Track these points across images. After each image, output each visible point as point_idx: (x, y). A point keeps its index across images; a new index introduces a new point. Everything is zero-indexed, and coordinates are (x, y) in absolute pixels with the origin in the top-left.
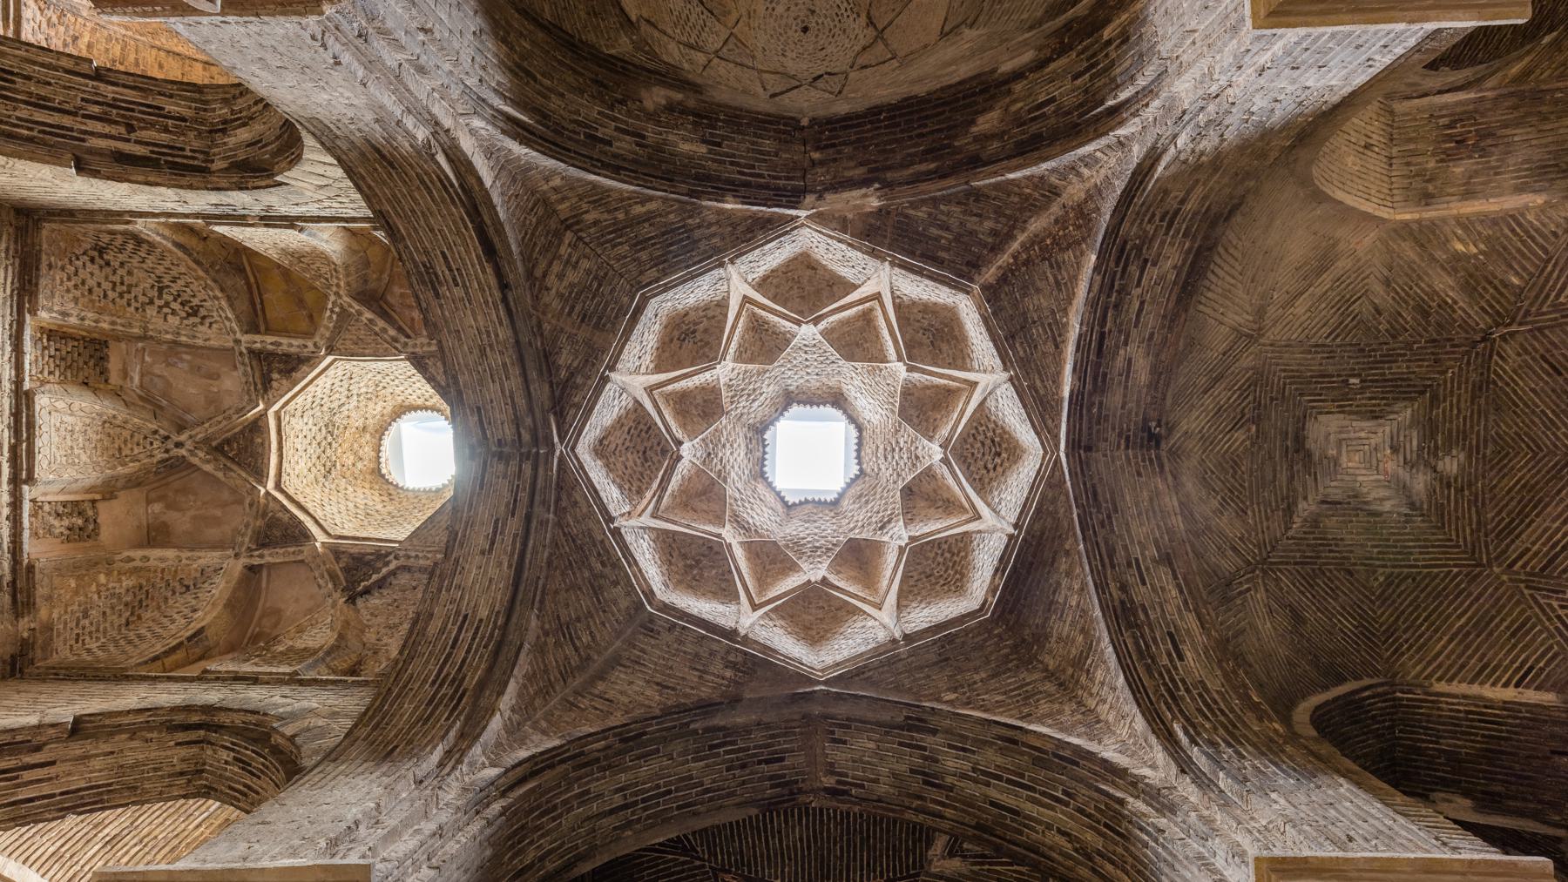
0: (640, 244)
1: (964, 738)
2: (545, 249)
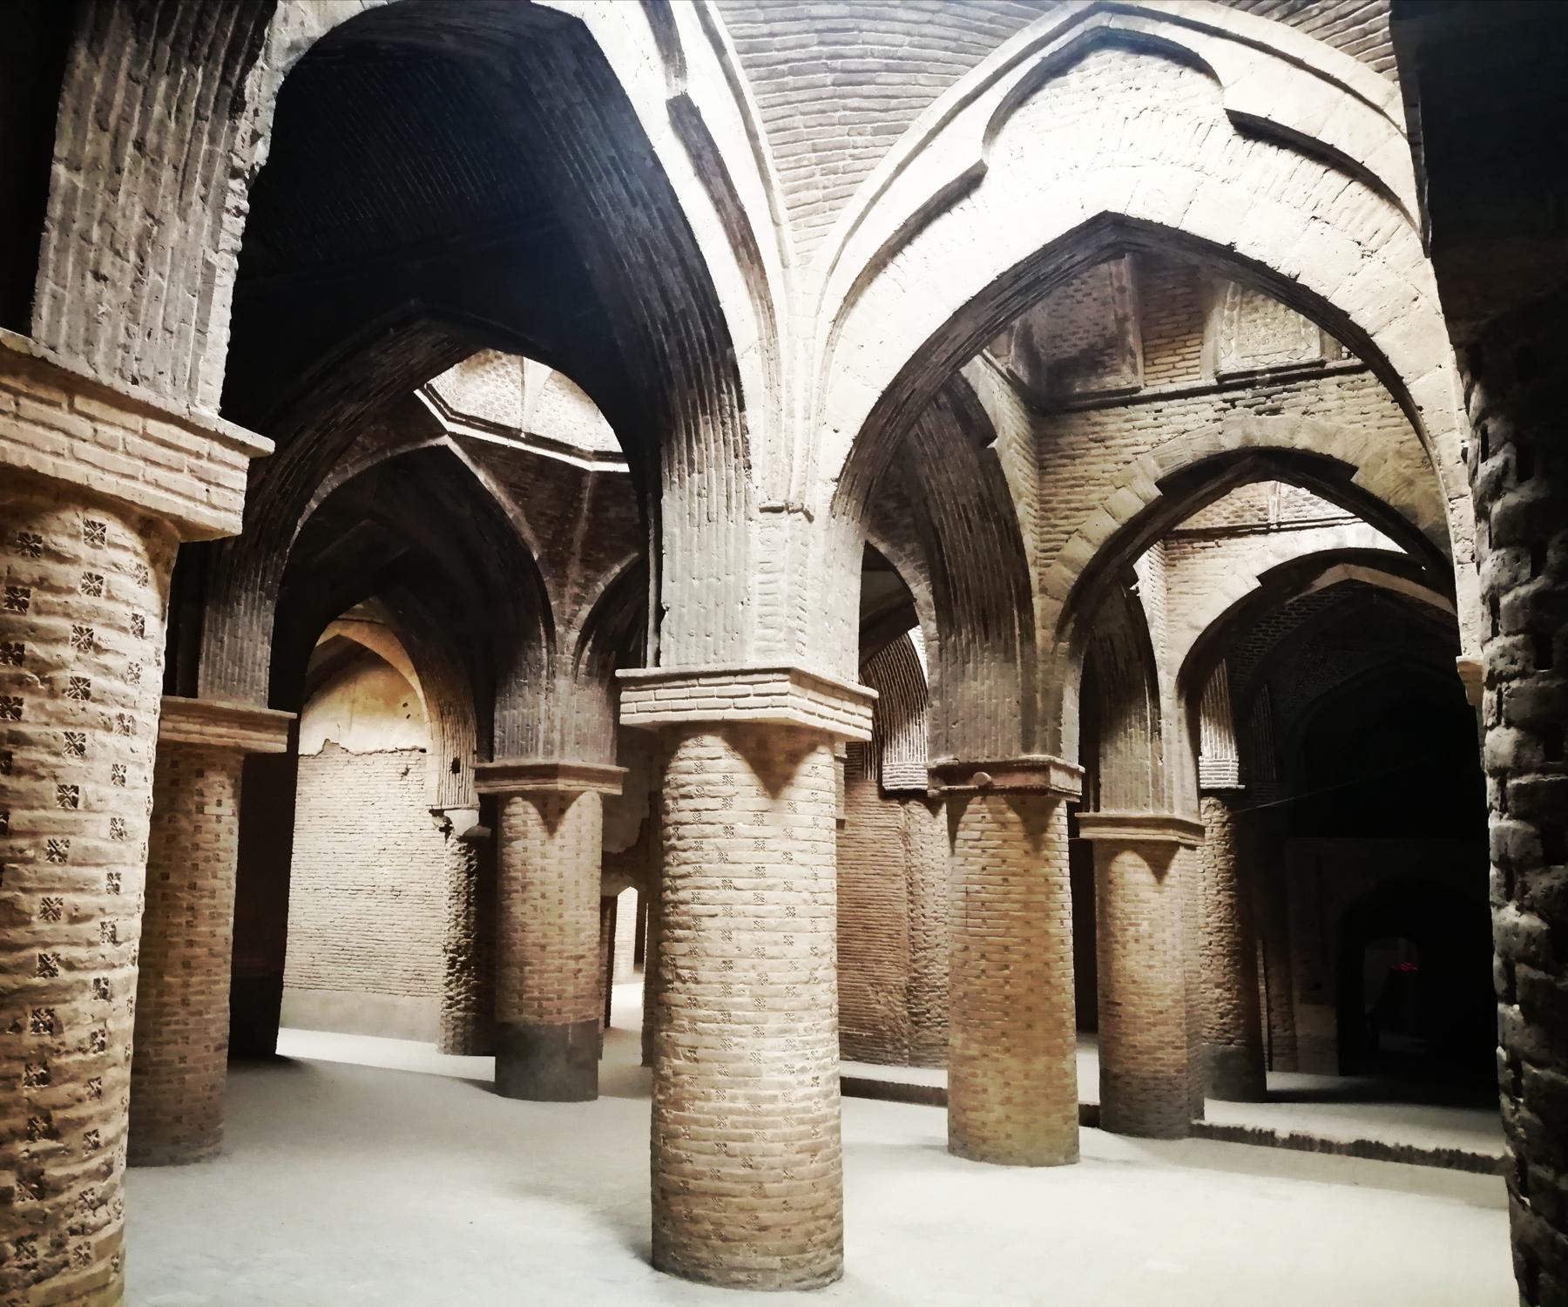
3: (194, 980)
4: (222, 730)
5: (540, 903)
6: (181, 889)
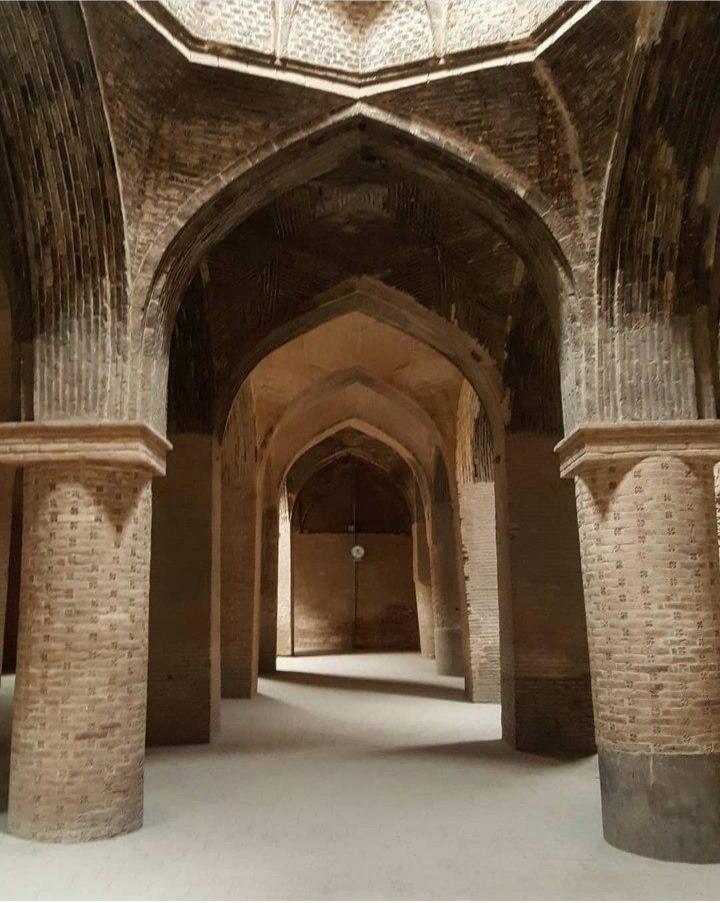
1: (83, 123)
3: (52, 672)
4: (65, 446)
5: (602, 598)
6: (39, 589)
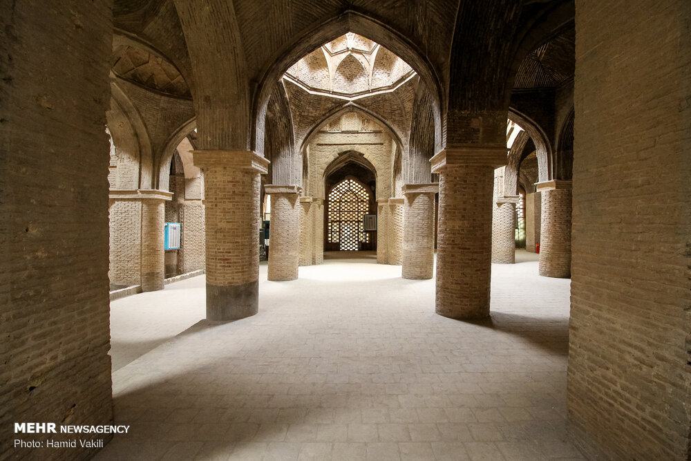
0: (300, 101)
2: (307, 118)
